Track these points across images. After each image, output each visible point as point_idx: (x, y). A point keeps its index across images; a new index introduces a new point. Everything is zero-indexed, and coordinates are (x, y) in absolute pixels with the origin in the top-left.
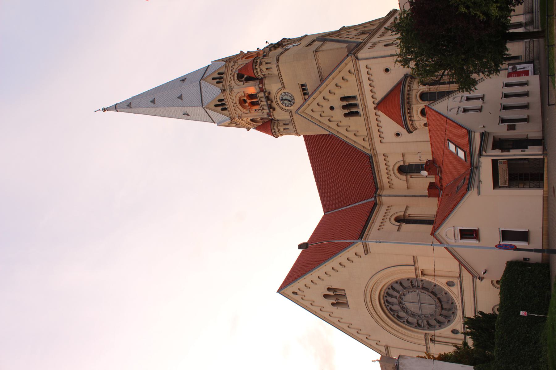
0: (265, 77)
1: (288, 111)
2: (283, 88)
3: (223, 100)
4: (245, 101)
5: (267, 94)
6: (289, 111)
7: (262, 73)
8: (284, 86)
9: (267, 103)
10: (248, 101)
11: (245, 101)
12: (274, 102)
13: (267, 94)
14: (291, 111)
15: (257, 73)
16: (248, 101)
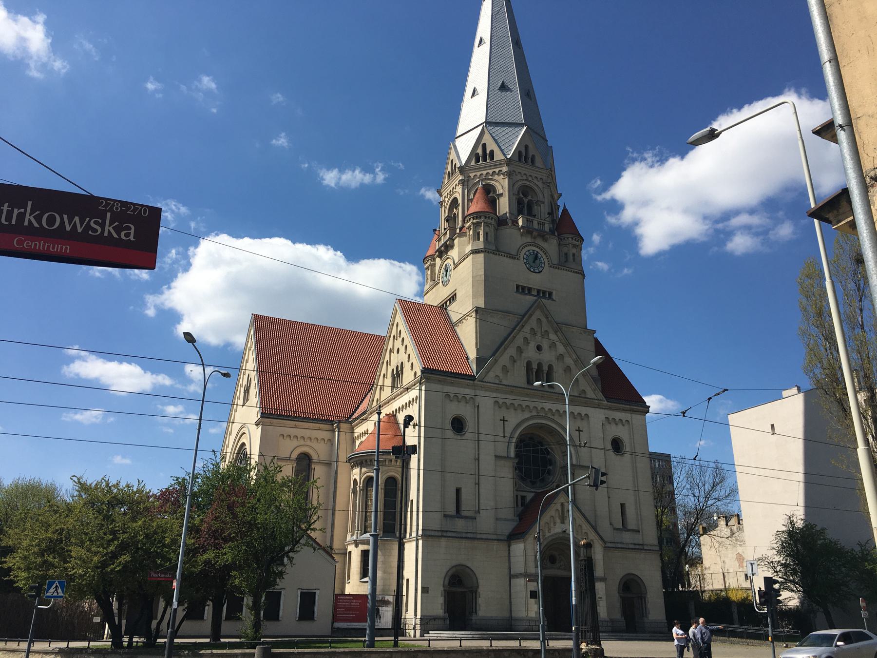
3: (533, 162)
4: (525, 195)
10: (526, 200)
11: (525, 195)
12: (533, 241)
14: (518, 259)
16: (526, 200)
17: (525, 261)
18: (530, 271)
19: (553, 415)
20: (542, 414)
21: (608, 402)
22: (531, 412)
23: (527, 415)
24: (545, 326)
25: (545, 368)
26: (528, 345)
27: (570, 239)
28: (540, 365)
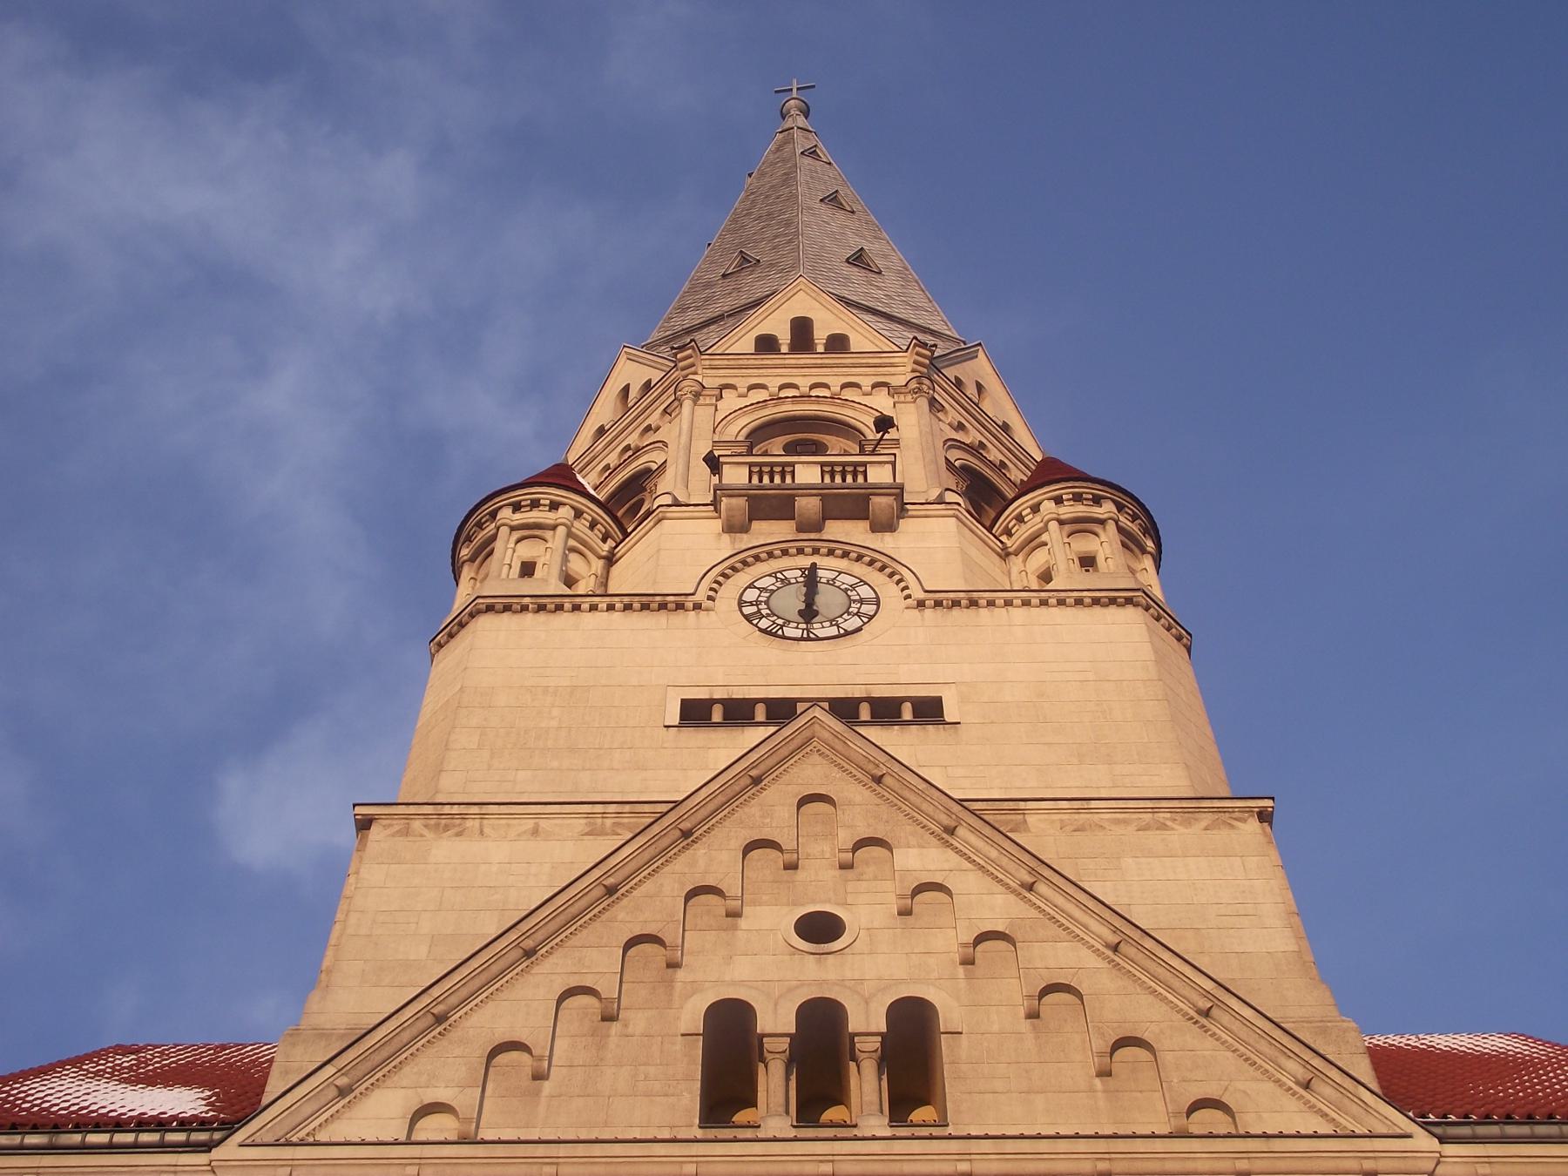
0: (1005, 554)
1: (701, 596)
2: (922, 595)
6: (701, 596)
7: (1053, 525)
8: (938, 604)
9: (808, 488)
13: (880, 503)
14: (697, 607)
15: (1058, 501)
17: (748, 610)
18: (784, 637)
26: (735, 928)
27: (1048, 507)
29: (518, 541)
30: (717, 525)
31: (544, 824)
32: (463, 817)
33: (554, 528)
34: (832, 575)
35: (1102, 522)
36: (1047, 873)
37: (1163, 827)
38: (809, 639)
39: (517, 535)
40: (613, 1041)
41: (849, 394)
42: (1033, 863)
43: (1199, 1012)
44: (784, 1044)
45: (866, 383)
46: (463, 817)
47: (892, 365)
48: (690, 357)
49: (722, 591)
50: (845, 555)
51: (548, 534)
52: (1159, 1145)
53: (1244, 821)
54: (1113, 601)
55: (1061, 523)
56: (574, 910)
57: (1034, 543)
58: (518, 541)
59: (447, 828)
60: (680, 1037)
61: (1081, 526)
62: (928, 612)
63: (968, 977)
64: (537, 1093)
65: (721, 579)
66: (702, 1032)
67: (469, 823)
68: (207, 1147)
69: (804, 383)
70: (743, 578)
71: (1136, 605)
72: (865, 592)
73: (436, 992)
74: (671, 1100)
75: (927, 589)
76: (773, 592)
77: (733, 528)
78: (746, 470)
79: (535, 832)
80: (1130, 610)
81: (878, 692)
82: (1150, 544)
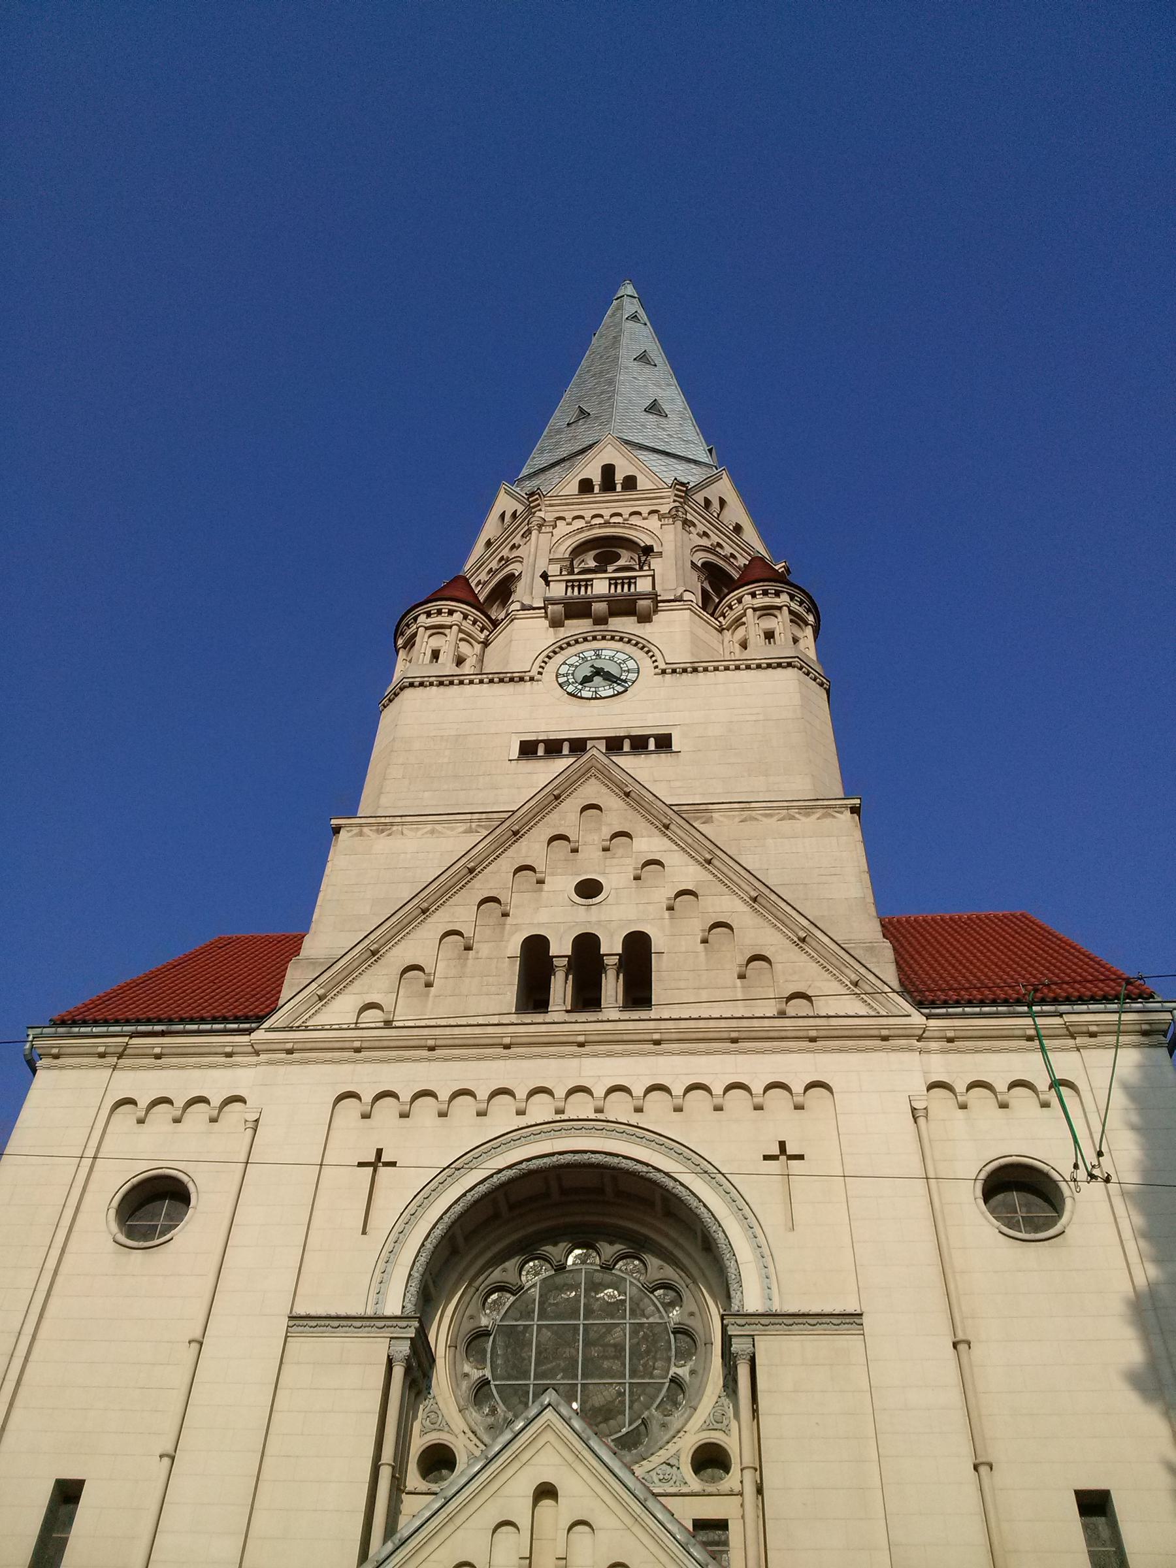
0: (721, 630)
1: (536, 669)
2: (662, 666)
5: (643, 604)
6: (534, 673)
7: (750, 611)
8: (674, 671)
9: (600, 598)
13: (643, 604)
14: (532, 679)
15: (754, 595)
17: (561, 680)
18: (581, 698)
19: (639, 1110)
20: (580, 1107)
21: (928, 1017)
22: (521, 1113)
23: (503, 1118)
24: (617, 814)
25: (611, 945)
26: (541, 890)
27: (747, 599)
28: (586, 944)
29: (430, 636)
30: (546, 623)
31: (438, 827)
32: (392, 824)
33: (450, 627)
34: (612, 653)
35: (779, 608)
36: (719, 853)
37: (792, 818)
38: (596, 698)
39: (429, 632)
40: (470, 962)
41: (635, 520)
42: (712, 847)
43: (799, 939)
44: (565, 961)
45: (645, 511)
46: (392, 824)
47: (661, 498)
48: (537, 499)
49: (547, 667)
50: (621, 639)
51: (447, 631)
52: (766, 1023)
53: (841, 813)
54: (779, 665)
55: (755, 610)
56: (450, 884)
57: (738, 622)
58: (430, 636)
59: (383, 831)
60: (507, 959)
61: (767, 611)
62: (668, 677)
63: (671, 918)
64: (427, 995)
65: (546, 660)
66: (519, 955)
67: (395, 828)
68: (249, 1032)
69: (606, 513)
70: (559, 658)
71: (794, 667)
72: (631, 664)
73: (372, 937)
74: (500, 997)
75: (667, 662)
76: (577, 666)
77: (556, 623)
78: (563, 585)
79: (432, 832)
80: (790, 669)
81: (634, 733)
82: (811, 618)
